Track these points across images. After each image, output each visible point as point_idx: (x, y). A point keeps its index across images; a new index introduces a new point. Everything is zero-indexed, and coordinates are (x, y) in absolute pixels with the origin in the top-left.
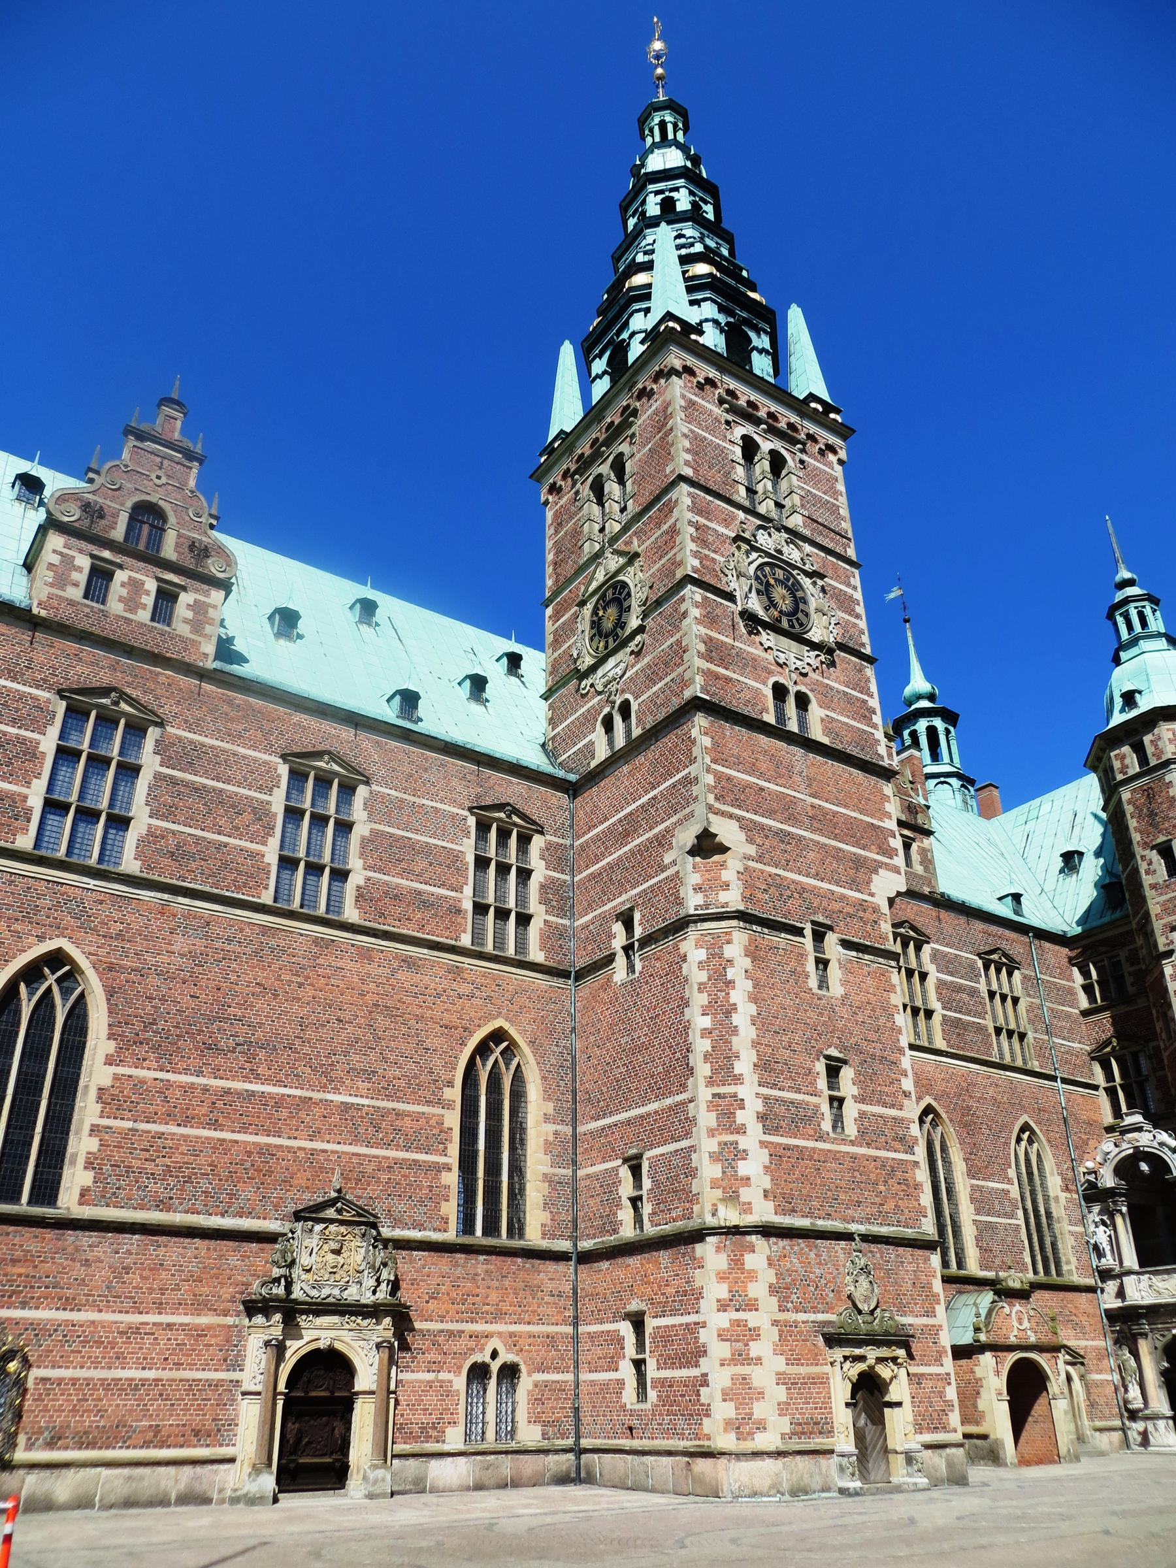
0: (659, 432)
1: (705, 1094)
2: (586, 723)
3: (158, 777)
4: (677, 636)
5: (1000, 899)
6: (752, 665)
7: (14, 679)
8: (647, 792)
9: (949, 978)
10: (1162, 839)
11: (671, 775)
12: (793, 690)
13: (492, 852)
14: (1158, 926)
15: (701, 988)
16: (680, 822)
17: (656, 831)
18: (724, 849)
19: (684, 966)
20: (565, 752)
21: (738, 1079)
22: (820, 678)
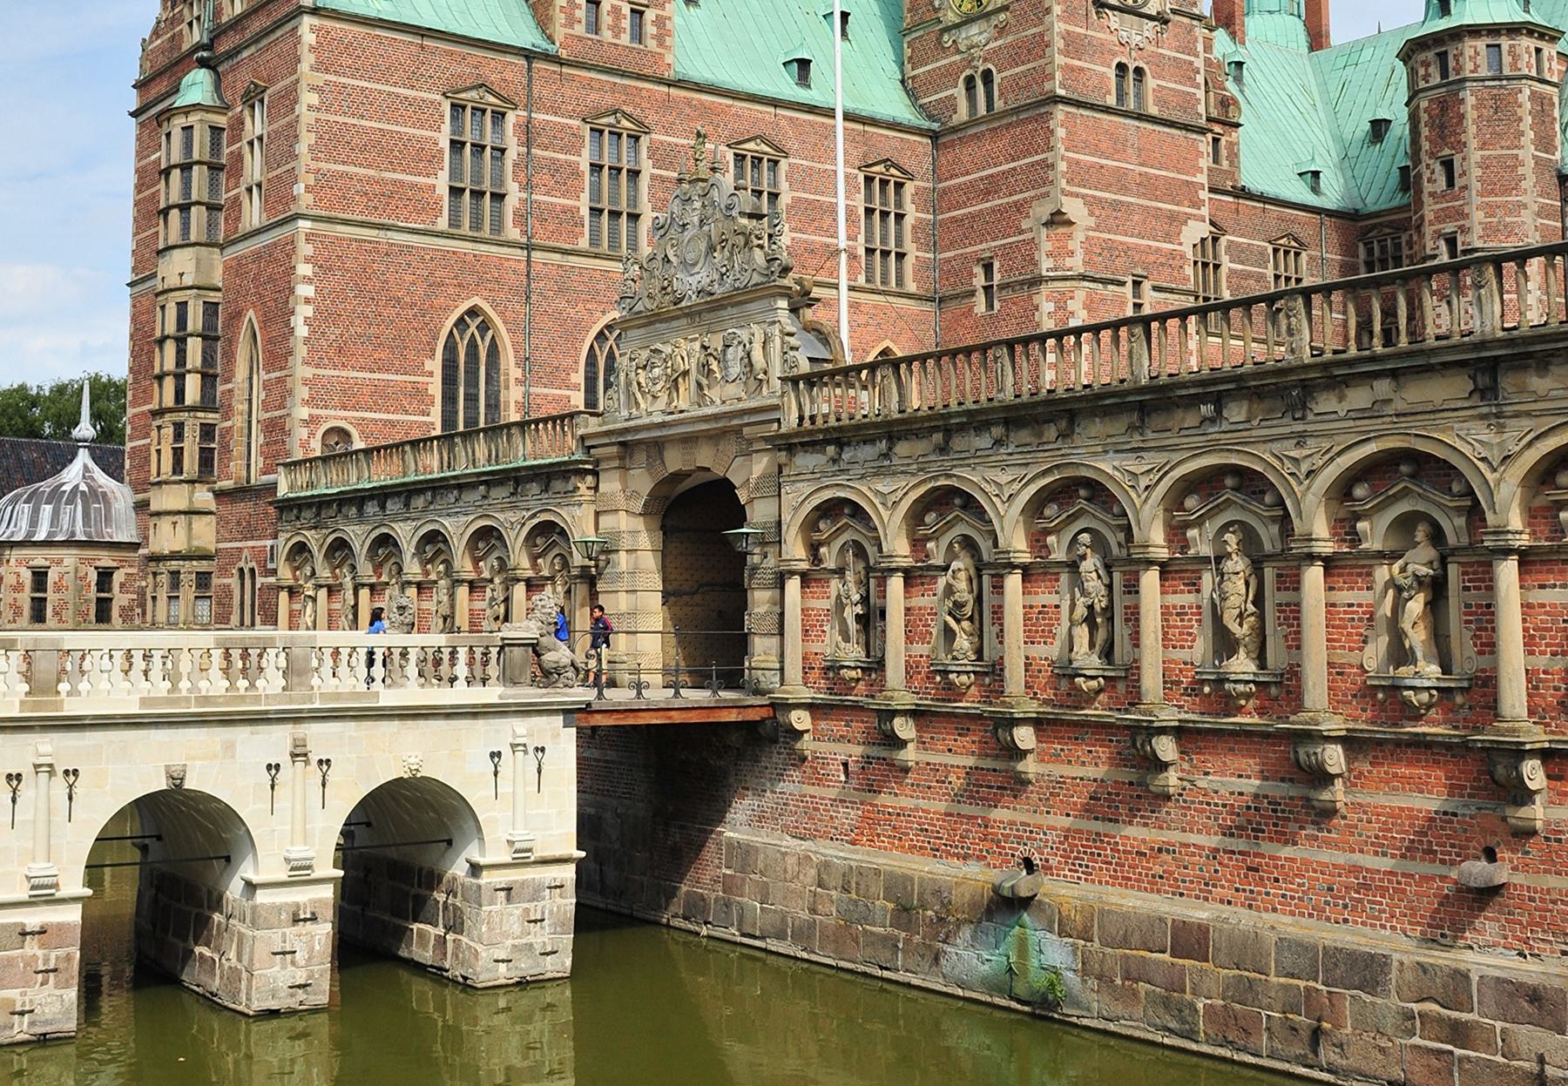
2: (949, 75)
3: (653, 177)
4: (1040, 29)
5: (1300, 175)
6: (1101, 51)
7: (556, 114)
9: (1240, 267)
10: (1447, 151)
11: (1030, 155)
12: (1131, 68)
13: (877, 205)
14: (1428, 230)
16: (1037, 198)
17: (1015, 198)
18: (1070, 223)
20: (926, 96)
22: (1154, 49)
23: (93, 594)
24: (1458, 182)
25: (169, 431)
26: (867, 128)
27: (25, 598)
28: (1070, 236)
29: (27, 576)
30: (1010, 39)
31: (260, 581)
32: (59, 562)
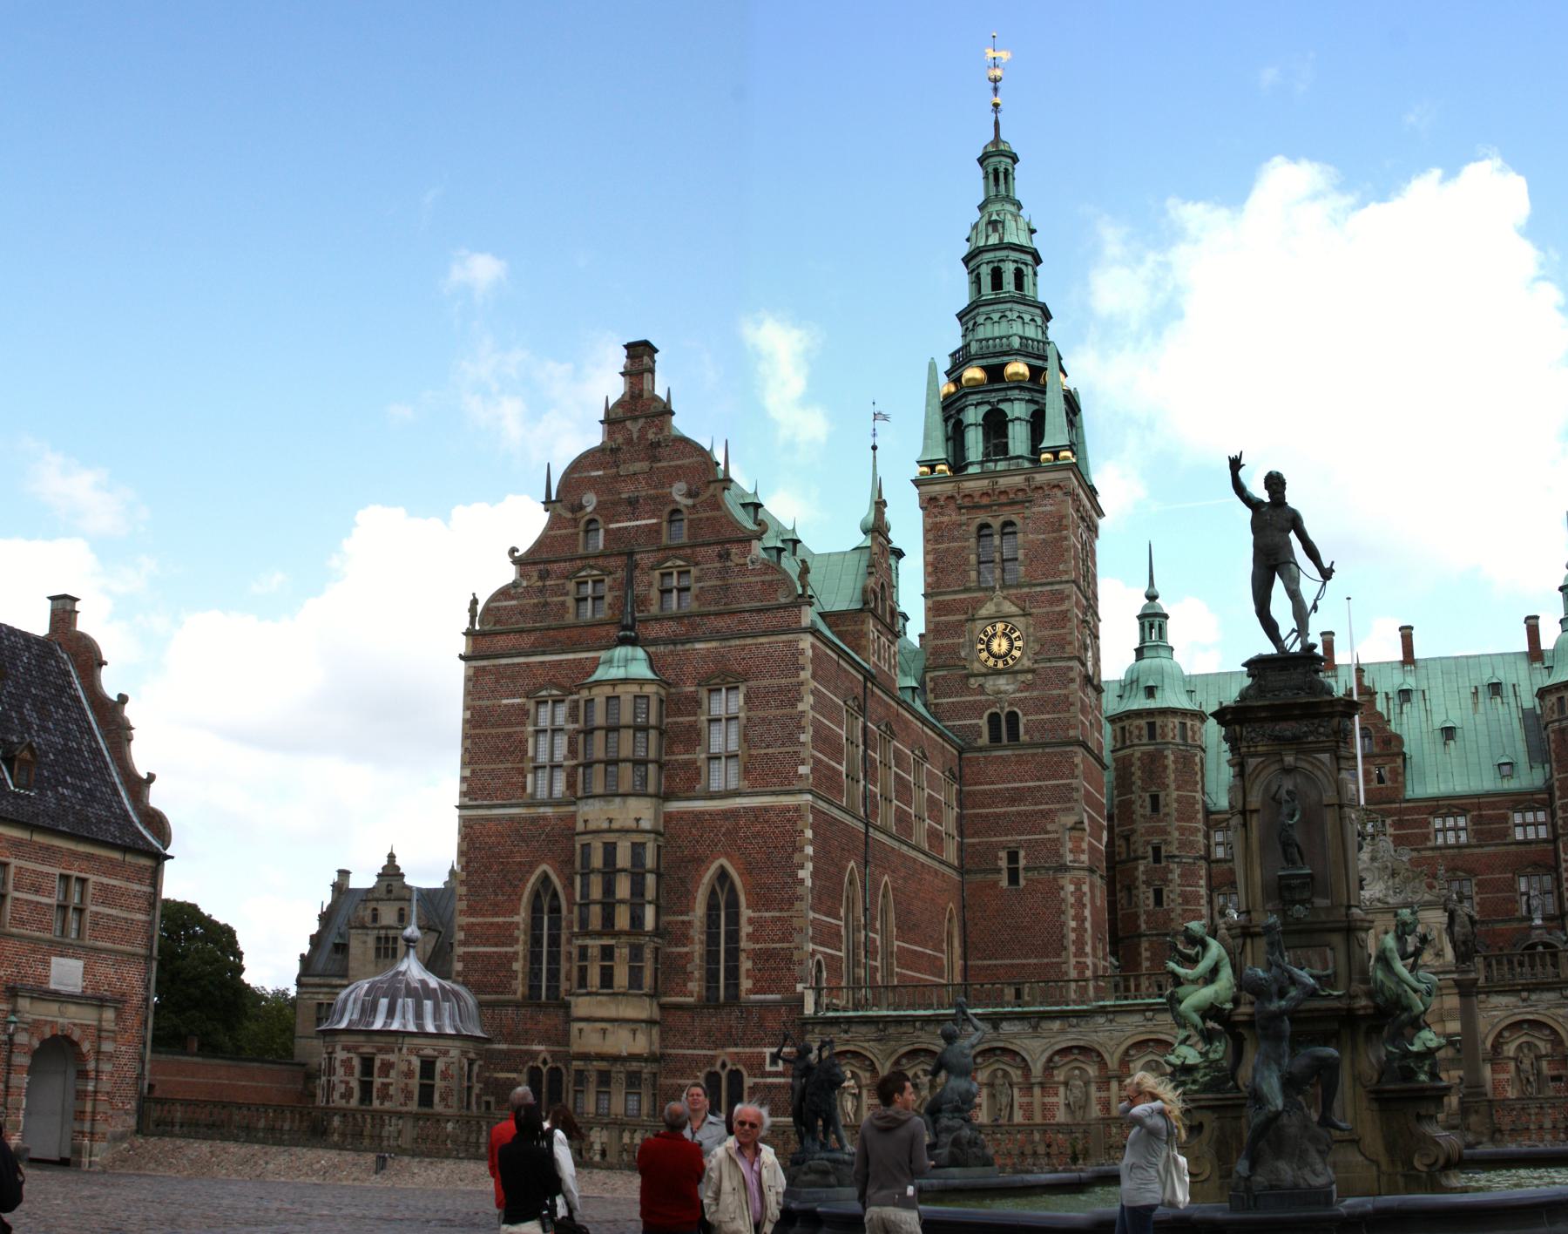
0: (1053, 532)
1: (1073, 961)
4: (1063, 692)
8: (1032, 780)
10: (1154, 789)
11: (1056, 779)
15: (1072, 907)
19: (1062, 893)
20: (948, 720)
21: (1086, 955)
23: (466, 1084)
24: (1163, 810)
25: (622, 953)
26: (946, 745)
27: (415, 1083)
28: (1082, 839)
29: (416, 1062)
30: (1035, 693)
31: (748, 1082)
32: (446, 1053)
